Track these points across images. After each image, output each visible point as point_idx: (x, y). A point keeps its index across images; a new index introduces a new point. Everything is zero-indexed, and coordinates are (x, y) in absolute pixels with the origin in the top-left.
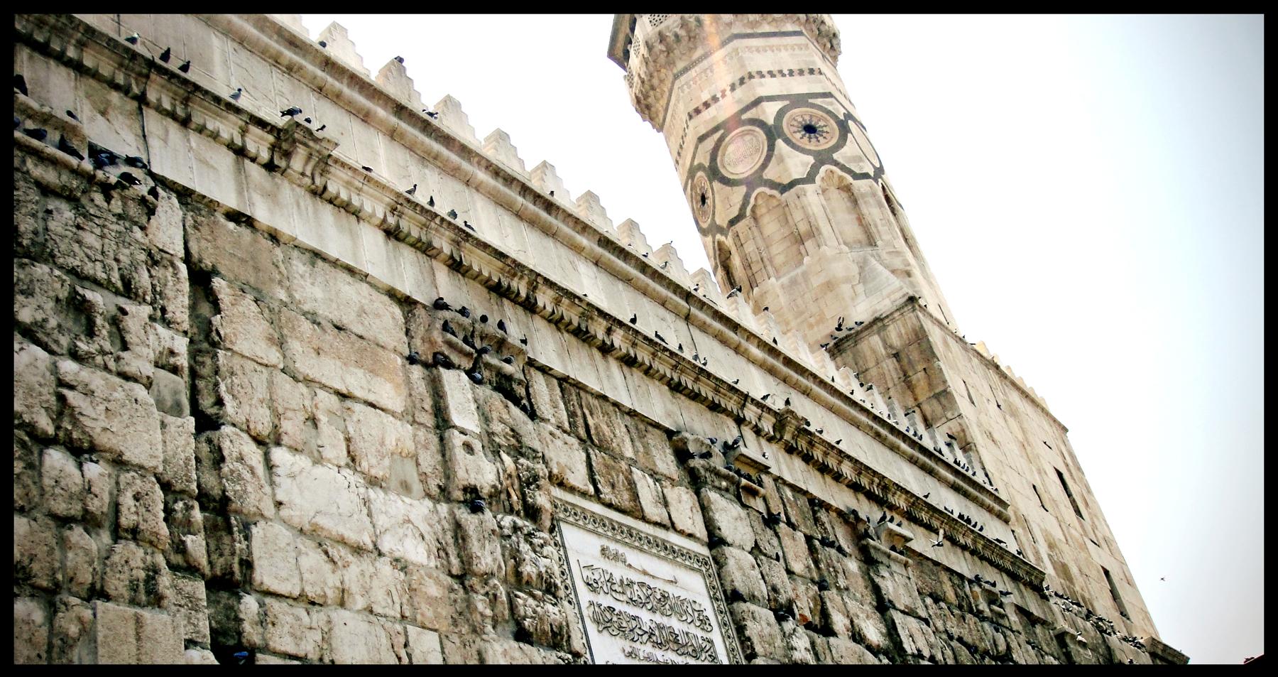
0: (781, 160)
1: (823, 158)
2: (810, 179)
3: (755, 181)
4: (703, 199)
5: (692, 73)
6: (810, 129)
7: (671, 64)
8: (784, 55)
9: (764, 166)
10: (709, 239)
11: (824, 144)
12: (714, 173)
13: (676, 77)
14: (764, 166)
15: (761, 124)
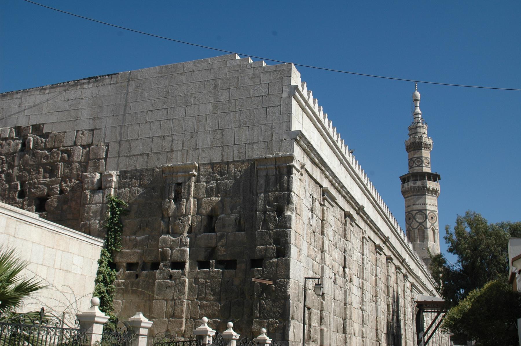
0: (427, 223)
1: (432, 224)
2: (429, 228)
3: (421, 224)
4: (410, 219)
5: (416, 197)
6: (432, 218)
7: (413, 192)
8: (432, 201)
9: (423, 222)
10: (408, 226)
11: (433, 221)
12: (414, 218)
13: (413, 195)
14: (423, 222)
15: (426, 214)
